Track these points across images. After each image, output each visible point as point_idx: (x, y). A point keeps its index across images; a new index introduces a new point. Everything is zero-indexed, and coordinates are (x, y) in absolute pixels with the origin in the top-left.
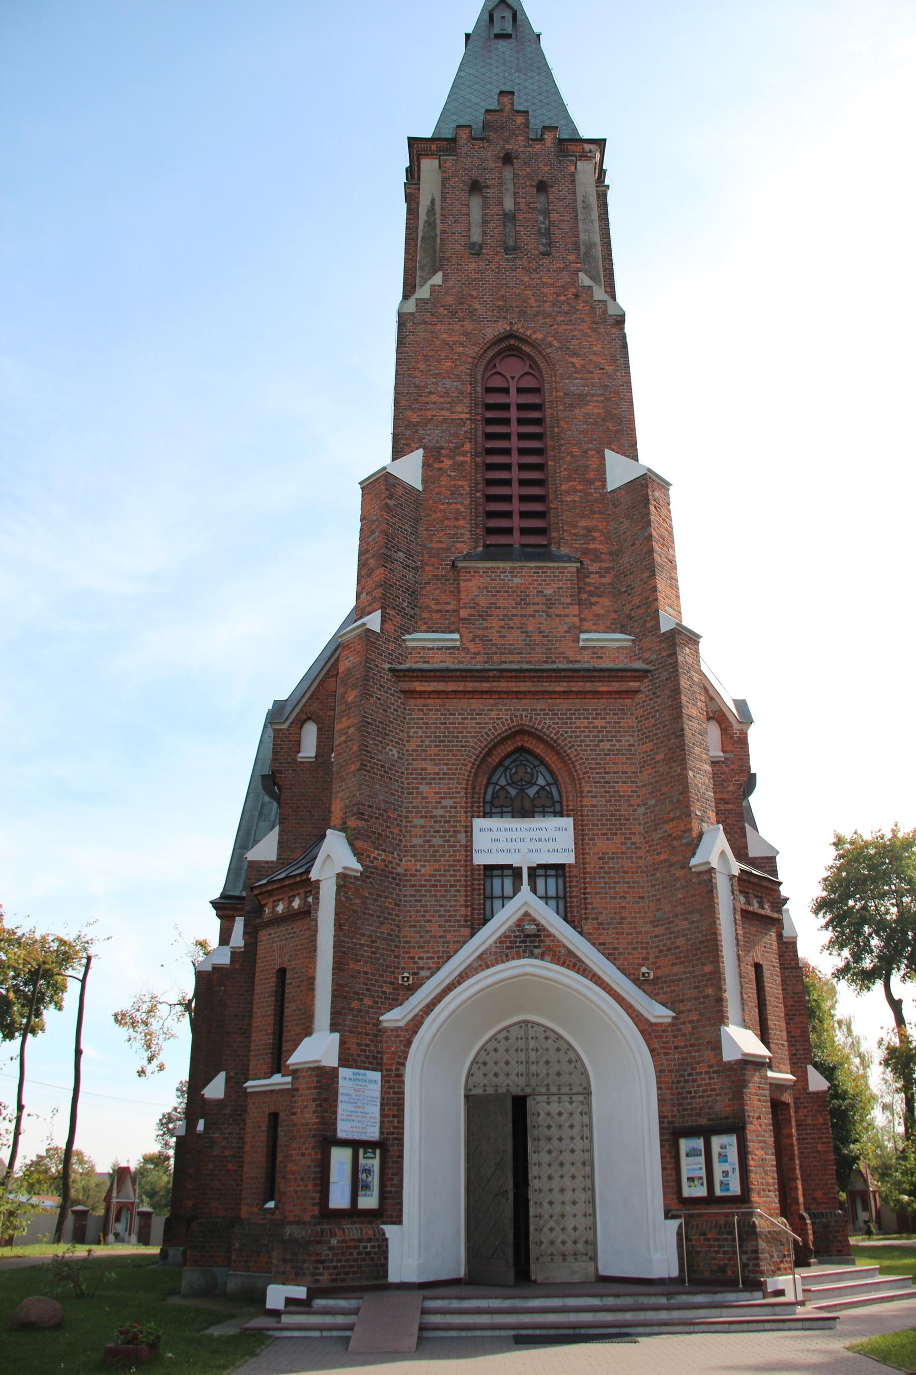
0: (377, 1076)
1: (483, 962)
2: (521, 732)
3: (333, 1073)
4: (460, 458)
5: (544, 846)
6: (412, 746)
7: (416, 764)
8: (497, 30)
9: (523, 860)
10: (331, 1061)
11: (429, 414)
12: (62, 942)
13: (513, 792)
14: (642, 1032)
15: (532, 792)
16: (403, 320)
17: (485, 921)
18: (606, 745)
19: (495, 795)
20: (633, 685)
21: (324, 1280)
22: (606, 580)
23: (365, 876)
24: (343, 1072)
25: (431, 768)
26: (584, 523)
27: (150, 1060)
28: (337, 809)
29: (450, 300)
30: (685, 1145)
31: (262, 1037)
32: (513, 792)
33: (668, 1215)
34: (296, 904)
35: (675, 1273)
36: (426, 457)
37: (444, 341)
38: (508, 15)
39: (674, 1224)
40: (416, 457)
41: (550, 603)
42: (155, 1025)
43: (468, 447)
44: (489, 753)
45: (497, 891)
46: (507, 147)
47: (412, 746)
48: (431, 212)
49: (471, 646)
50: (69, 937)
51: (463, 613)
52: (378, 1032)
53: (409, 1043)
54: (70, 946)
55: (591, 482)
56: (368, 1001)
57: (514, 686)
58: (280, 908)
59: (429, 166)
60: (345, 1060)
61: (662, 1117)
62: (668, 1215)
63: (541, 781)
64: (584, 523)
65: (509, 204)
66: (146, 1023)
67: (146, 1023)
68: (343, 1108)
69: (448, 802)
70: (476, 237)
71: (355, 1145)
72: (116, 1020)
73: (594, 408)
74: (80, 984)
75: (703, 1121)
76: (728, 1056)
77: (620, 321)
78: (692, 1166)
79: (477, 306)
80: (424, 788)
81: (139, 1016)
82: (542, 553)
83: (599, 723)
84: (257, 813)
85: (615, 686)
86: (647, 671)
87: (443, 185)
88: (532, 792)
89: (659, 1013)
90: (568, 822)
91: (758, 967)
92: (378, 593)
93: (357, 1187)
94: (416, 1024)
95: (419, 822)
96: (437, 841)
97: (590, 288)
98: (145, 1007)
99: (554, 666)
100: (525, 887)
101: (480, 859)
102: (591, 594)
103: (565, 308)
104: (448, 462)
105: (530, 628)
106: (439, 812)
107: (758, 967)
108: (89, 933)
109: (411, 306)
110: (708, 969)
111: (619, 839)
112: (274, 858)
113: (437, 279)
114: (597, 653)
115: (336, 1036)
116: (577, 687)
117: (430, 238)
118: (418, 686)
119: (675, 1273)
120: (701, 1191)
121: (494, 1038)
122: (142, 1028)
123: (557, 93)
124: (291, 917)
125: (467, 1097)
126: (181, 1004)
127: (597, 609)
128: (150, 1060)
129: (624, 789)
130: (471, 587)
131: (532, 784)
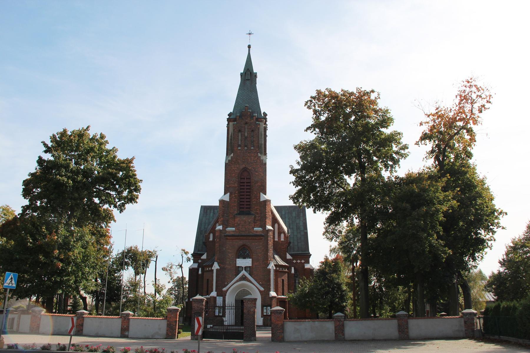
0: (222, 297)
1: (237, 281)
2: (244, 245)
5: (247, 263)
6: (227, 247)
7: (228, 250)
8: (247, 79)
9: (244, 266)
10: (216, 296)
11: (230, 185)
12: (150, 252)
15: (246, 254)
16: (226, 165)
17: (238, 274)
18: (257, 248)
19: (240, 255)
20: (262, 238)
22: (259, 218)
23: (220, 269)
24: (217, 297)
25: (230, 251)
26: (256, 207)
27: (171, 279)
28: (216, 260)
29: (234, 160)
30: (264, 308)
31: (205, 289)
33: (262, 317)
34: (210, 269)
35: (262, 325)
37: (233, 169)
38: (249, 73)
39: (262, 318)
40: (228, 194)
41: (250, 223)
42: (172, 270)
43: (237, 192)
45: (240, 270)
47: (227, 247)
48: (231, 136)
49: (237, 230)
50: (152, 251)
51: (236, 225)
53: (226, 293)
54: (152, 253)
55: (258, 199)
58: (207, 269)
59: (231, 124)
60: (218, 295)
62: (262, 317)
63: (247, 252)
64: (256, 207)
65: (246, 135)
66: (170, 270)
67: (170, 270)
69: (233, 257)
70: (240, 143)
71: (219, 307)
72: (162, 269)
73: (259, 184)
74: (155, 262)
75: (267, 305)
76: (270, 296)
77: (265, 164)
78: (265, 311)
79: (239, 161)
80: (229, 254)
81: (168, 268)
82: (249, 214)
83: (256, 244)
84: (200, 233)
85: (259, 238)
86: (264, 236)
87: (234, 131)
88: (246, 254)
89: (262, 289)
90: (251, 260)
91: (283, 280)
92: (222, 222)
93: (219, 312)
94: (227, 290)
95: (228, 260)
96: (231, 263)
97: (260, 157)
98: (170, 266)
100: (244, 270)
101: (237, 265)
102: (257, 221)
103: (255, 161)
104: (234, 195)
106: (231, 258)
107: (283, 280)
108: (156, 249)
109: (227, 162)
110: (269, 284)
111: (258, 263)
112: (206, 258)
113: (232, 155)
114: (257, 232)
116: (253, 238)
117: (231, 143)
118: (228, 238)
119: (262, 325)
120: (266, 314)
124: (209, 271)
125: (235, 300)
126: (179, 265)
127: (257, 224)
128: (171, 279)
129: (260, 255)
130: (237, 220)
131: (246, 253)
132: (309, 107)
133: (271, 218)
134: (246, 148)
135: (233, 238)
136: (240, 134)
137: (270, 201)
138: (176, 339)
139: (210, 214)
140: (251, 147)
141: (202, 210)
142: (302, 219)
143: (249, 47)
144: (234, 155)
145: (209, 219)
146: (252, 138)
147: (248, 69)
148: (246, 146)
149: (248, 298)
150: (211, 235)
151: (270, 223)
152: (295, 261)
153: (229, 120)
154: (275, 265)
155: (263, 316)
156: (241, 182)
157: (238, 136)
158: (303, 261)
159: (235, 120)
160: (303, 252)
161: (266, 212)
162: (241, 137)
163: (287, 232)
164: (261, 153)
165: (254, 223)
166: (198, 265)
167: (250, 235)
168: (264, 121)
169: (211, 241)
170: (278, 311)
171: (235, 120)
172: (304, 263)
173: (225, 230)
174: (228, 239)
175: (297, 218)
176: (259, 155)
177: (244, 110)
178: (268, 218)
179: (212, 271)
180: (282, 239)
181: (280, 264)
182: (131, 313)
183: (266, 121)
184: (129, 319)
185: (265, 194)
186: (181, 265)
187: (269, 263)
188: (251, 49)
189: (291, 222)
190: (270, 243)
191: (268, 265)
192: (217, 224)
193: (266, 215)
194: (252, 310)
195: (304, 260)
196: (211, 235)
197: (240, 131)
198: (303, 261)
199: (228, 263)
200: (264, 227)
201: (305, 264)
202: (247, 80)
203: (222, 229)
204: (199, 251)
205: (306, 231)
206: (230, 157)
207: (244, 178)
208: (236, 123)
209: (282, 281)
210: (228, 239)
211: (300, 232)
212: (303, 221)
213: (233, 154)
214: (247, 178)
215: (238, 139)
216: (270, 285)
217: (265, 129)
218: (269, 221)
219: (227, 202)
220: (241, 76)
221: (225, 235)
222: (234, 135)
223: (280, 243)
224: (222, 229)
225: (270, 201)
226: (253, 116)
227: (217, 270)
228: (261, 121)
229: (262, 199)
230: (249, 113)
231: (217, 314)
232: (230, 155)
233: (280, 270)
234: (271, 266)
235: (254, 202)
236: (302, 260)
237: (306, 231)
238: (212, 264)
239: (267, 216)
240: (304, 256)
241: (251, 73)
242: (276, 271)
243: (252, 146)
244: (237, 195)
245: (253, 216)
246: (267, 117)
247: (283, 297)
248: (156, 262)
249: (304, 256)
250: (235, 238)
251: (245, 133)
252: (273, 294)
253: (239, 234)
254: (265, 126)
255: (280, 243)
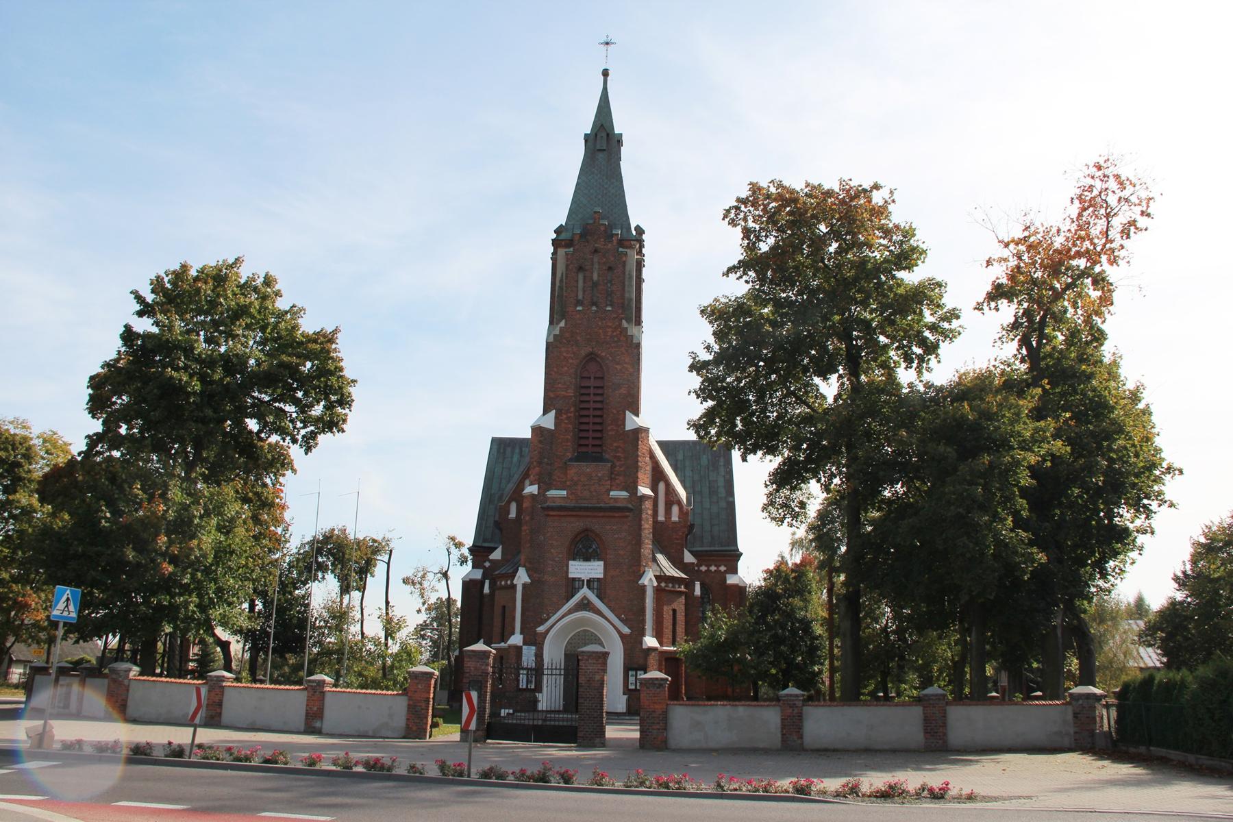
1: (570, 612)
2: (587, 530)
3: (521, 647)
4: (569, 415)
5: (593, 571)
8: (598, 147)
9: (585, 577)
10: (520, 643)
12: (374, 541)
13: (584, 550)
14: (621, 637)
15: (590, 551)
16: (548, 345)
17: (573, 596)
18: (616, 536)
19: (578, 551)
20: (627, 514)
21: (519, 708)
24: (524, 647)
26: (615, 444)
27: (424, 604)
28: (522, 562)
29: (567, 335)
30: (630, 673)
31: (497, 630)
32: (584, 550)
33: (624, 694)
34: (509, 582)
35: (625, 711)
36: (556, 413)
37: (565, 357)
38: (604, 135)
39: (626, 697)
40: (553, 413)
41: (600, 479)
42: (426, 584)
43: (572, 409)
44: (576, 537)
45: (577, 586)
46: (596, 245)
48: (561, 281)
50: (379, 538)
51: (568, 483)
52: (535, 633)
54: (380, 543)
56: (532, 625)
57: (585, 513)
58: (503, 583)
59: (561, 251)
60: (525, 643)
61: (624, 664)
62: (624, 694)
63: (594, 547)
64: (615, 444)
65: (595, 277)
68: (524, 658)
70: (580, 297)
71: (527, 669)
72: (404, 582)
73: (623, 391)
75: (636, 666)
77: (638, 346)
78: (632, 680)
79: (579, 338)
81: (416, 580)
82: (598, 458)
85: (620, 514)
86: (632, 510)
87: (567, 270)
88: (590, 551)
89: (626, 630)
90: (602, 563)
91: (674, 611)
92: (537, 477)
93: (528, 682)
94: (547, 631)
96: (556, 569)
97: (627, 328)
98: (420, 575)
99: (599, 505)
100: (585, 586)
101: (571, 576)
102: (616, 475)
103: (616, 339)
104: (565, 416)
105: (592, 490)
106: (557, 559)
107: (674, 611)
108: (388, 536)
109: (551, 340)
111: (618, 570)
113: (562, 324)
114: (616, 500)
115: (522, 636)
116: (607, 514)
117: (561, 296)
118: (551, 513)
119: (625, 711)
120: (633, 687)
121: (574, 635)
122: (418, 586)
123: (624, 196)
124: (507, 587)
125: (565, 654)
126: (440, 573)
129: (621, 552)
130: (572, 472)
131: (590, 547)
132: (733, 223)
133: (649, 468)
134: (594, 308)
135: (562, 513)
136: (581, 276)
137: (646, 430)
138: (428, 739)
139: (512, 457)
140: (607, 305)
141: (495, 447)
142: (722, 470)
143: (605, 73)
144: (566, 324)
145: (510, 469)
146: (609, 285)
147: (602, 125)
148: (594, 304)
149: (589, 652)
150: (513, 507)
151: (648, 481)
152: (703, 568)
153: (555, 243)
154: (656, 577)
155: (627, 691)
156: (583, 385)
157: (577, 281)
158: (723, 568)
159: (569, 243)
160: (722, 546)
161: (638, 456)
162: (584, 282)
163: (685, 501)
164: (629, 321)
165: (611, 479)
166: (484, 572)
167: (601, 508)
168: (638, 246)
169: (512, 520)
170: (656, 682)
171: (569, 243)
172: (726, 572)
173: (544, 495)
174: (548, 515)
175: (711, 468)
176: (625, 324)
177: (591, 222)
178: (643, 470)
179: (514, 587)
180: (675, 518)
181: (668, 574)
182: (328, 679)
183: (642, 246)
184: (323, 693)
185: (637, 415)
186: (446, 572)
187: (644, 572)
188: (609, 78)
189: (696, 477)
190: (647, 526)
191: (641, 576)
192: (527, 482)
193: (637, 461)
194: (597, 677)
195: (725, 566)
196: (513, 507)
197: (581, 269)
198: (723, 568)
199: (550, 569)
200: (633, 488)
201: (727, 575)
202: (599, 150)
203: (536, 493)
204: (485, 541)
205: (731, 499)
206: (558, 329)
207: (590, 378)
208: (571, 249)
209: (671, 613)
210: (548, 515)
211: (718, 502)
212: (724, 476)
213: (564, 321)
214: (595, 378)
215: (577, 287)
216: (643, 622)
217: (640, 265)
218: (644, 476)
219: (549, 430)
220: (586, 141)
221: (545, 505)
222: (567, 277)
223: (670, 526)
224: (536, 493)
225: (646, 430)
226: (612, 235)
227: (525, 586)
228: (631, 247)
229: (629, 427)
230: (602, 228)
231: (523, 685)
232: (557, 324)
233: (667, 588)
234: (648, 579)
235: (610, 433)
236: (720, 566)
237: (731, 499)
238: (513, 572)
239: (640, 464)
240: (724, 556)
241: (608, 135)
242: (658, 591)
243: (608, 303)
244: (572, 415)
245: (609, 464)
246: (644, 237)
247: (672, 648)
248: (388, 564)
249: (724, 556)
250: (565, 513)
251: (592, 274)
252: (650, 641)
253: (577, 505)
254: (638, 257)
255: (670, 526)
